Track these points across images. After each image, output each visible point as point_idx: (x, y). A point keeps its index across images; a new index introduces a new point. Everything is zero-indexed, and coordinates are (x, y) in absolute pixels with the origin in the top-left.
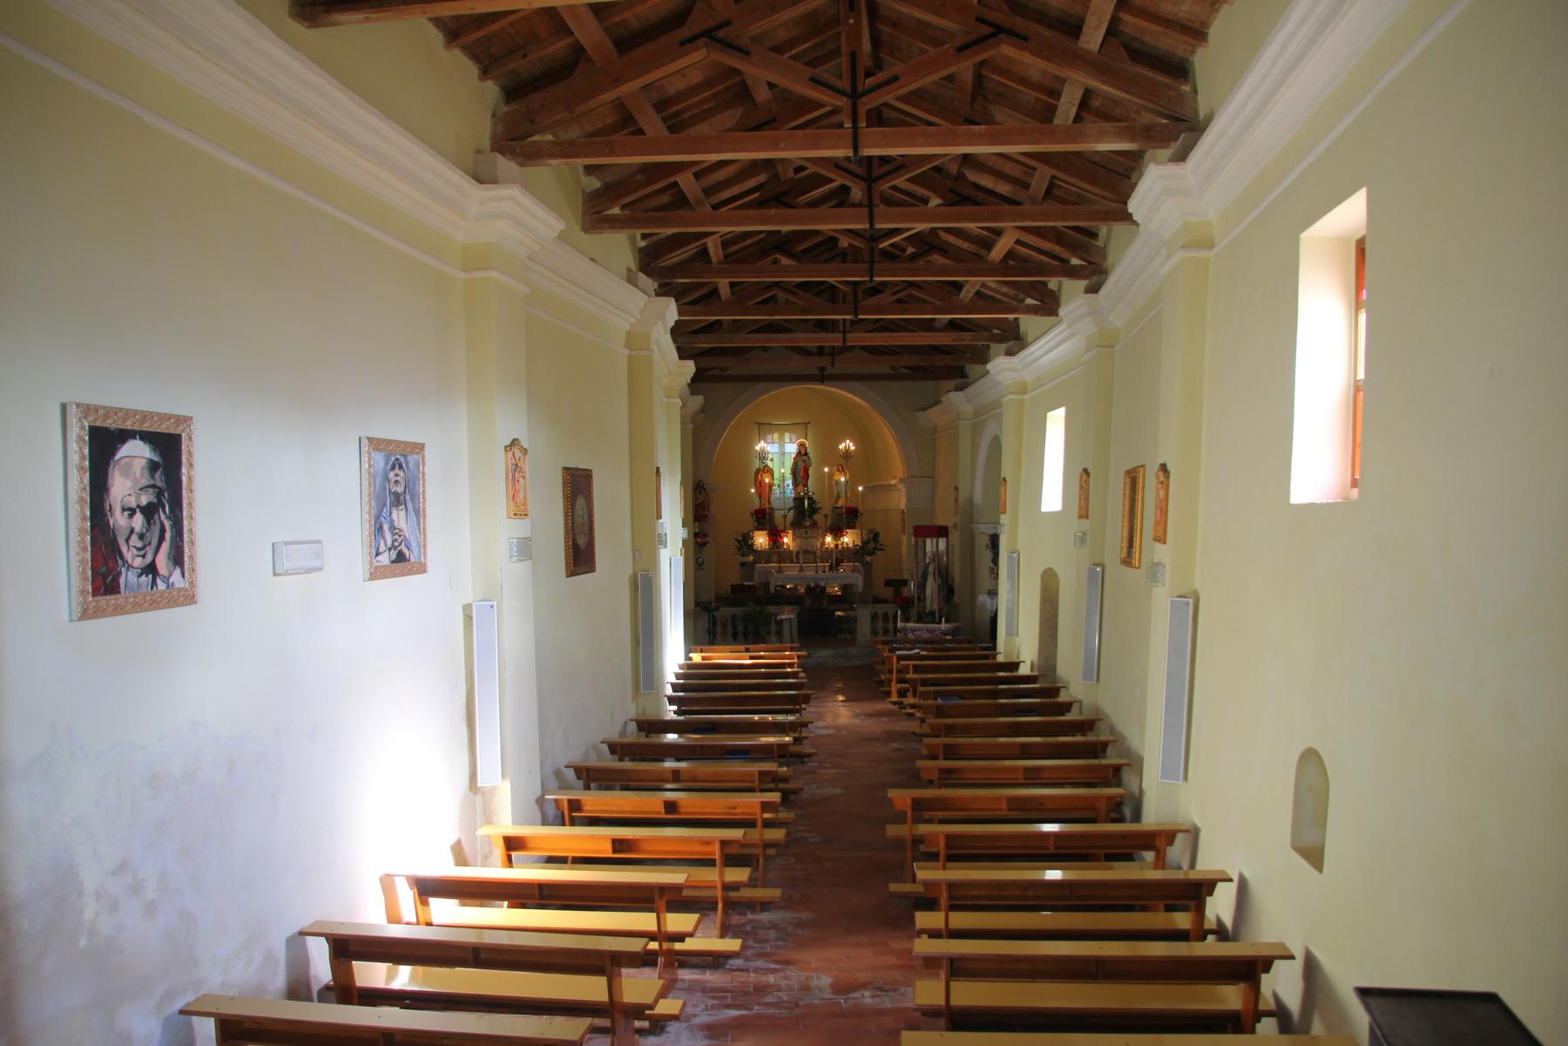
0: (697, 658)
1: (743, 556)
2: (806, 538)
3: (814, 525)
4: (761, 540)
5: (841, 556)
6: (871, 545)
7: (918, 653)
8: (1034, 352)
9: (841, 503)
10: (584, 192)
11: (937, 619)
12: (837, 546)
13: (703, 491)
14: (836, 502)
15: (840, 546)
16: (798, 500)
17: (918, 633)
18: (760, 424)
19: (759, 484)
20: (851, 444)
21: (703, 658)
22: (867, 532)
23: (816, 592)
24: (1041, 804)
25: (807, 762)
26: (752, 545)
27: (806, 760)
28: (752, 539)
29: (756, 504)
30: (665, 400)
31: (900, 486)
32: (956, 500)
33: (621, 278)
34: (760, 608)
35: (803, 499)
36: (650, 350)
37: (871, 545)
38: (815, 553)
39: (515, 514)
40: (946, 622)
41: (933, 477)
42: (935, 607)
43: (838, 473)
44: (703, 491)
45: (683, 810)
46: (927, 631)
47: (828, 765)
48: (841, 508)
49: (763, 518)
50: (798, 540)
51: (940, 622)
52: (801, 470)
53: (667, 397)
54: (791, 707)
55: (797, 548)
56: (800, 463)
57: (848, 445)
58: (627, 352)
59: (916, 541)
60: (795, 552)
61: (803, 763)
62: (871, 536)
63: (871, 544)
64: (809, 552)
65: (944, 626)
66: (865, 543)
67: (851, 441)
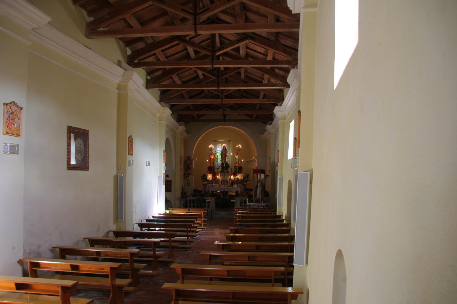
0: (168, 212)
1: (204, 181)
2: (225, 176)
3: (228, 172)
4: (210, 177)
5: (237, 182)
6: (246, 179)
7: (246, 212)
8: (285, 103)
9: (237, 165)
10: (87, 22)
11: (260, 202)
13: (189, 160)
14: (236, 165)
15: (236, 179)
16: (223, 164)
17: (254, 206)
18: (214, 141)
19: (210, 159)
20: (240, 146)
21: (170, 212)
22: (245, 174)
23: (225, 193)
24: (245, 274)
25: (188, 251)
26: (207, 178)
27: (188, 249)
28: (207, 176)
29: (209, 165)
30: (158, 121)
31: (256, 159)
32: (270, 162)
33: (114, 63)
34: (201, 197)
35: (224, 164)
36: (127, 91)
37: (246, 179)
39: (7, 133)
40: (264, 202)
41: (266, 156)
42: (260, 198)
43: (236, 155)
44: (189, 160)
45: (81, 269)
46: (257, 206)
47: (196, 252)
48: (237, 166)
49: (211, 170)
50: (222, 177)
51: (261, 203)
52: (224, 153)
53: (159, 120)
54: (186, 229)
55: (222, 180)
57: (239, 146)
58: (118, 91)
59: (254, 175)
61: (186, 250)
62: (246, 176)
63: (246, 178)
65: (262, 204)
66: (244, 178)
67: (240, 145)
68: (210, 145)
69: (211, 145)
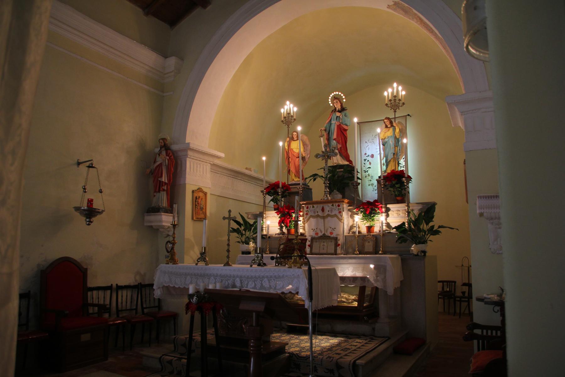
2: (324, 218)
12: (370, 228)
15: (376, 229)
20: (400, 88)
38: (336, 239)
55: (313, 234)
56: (333, 122)
60: (309, 238)
64: (328, 238)
67: (399, 84)
68: (285, 104)
69: (288, 103)
